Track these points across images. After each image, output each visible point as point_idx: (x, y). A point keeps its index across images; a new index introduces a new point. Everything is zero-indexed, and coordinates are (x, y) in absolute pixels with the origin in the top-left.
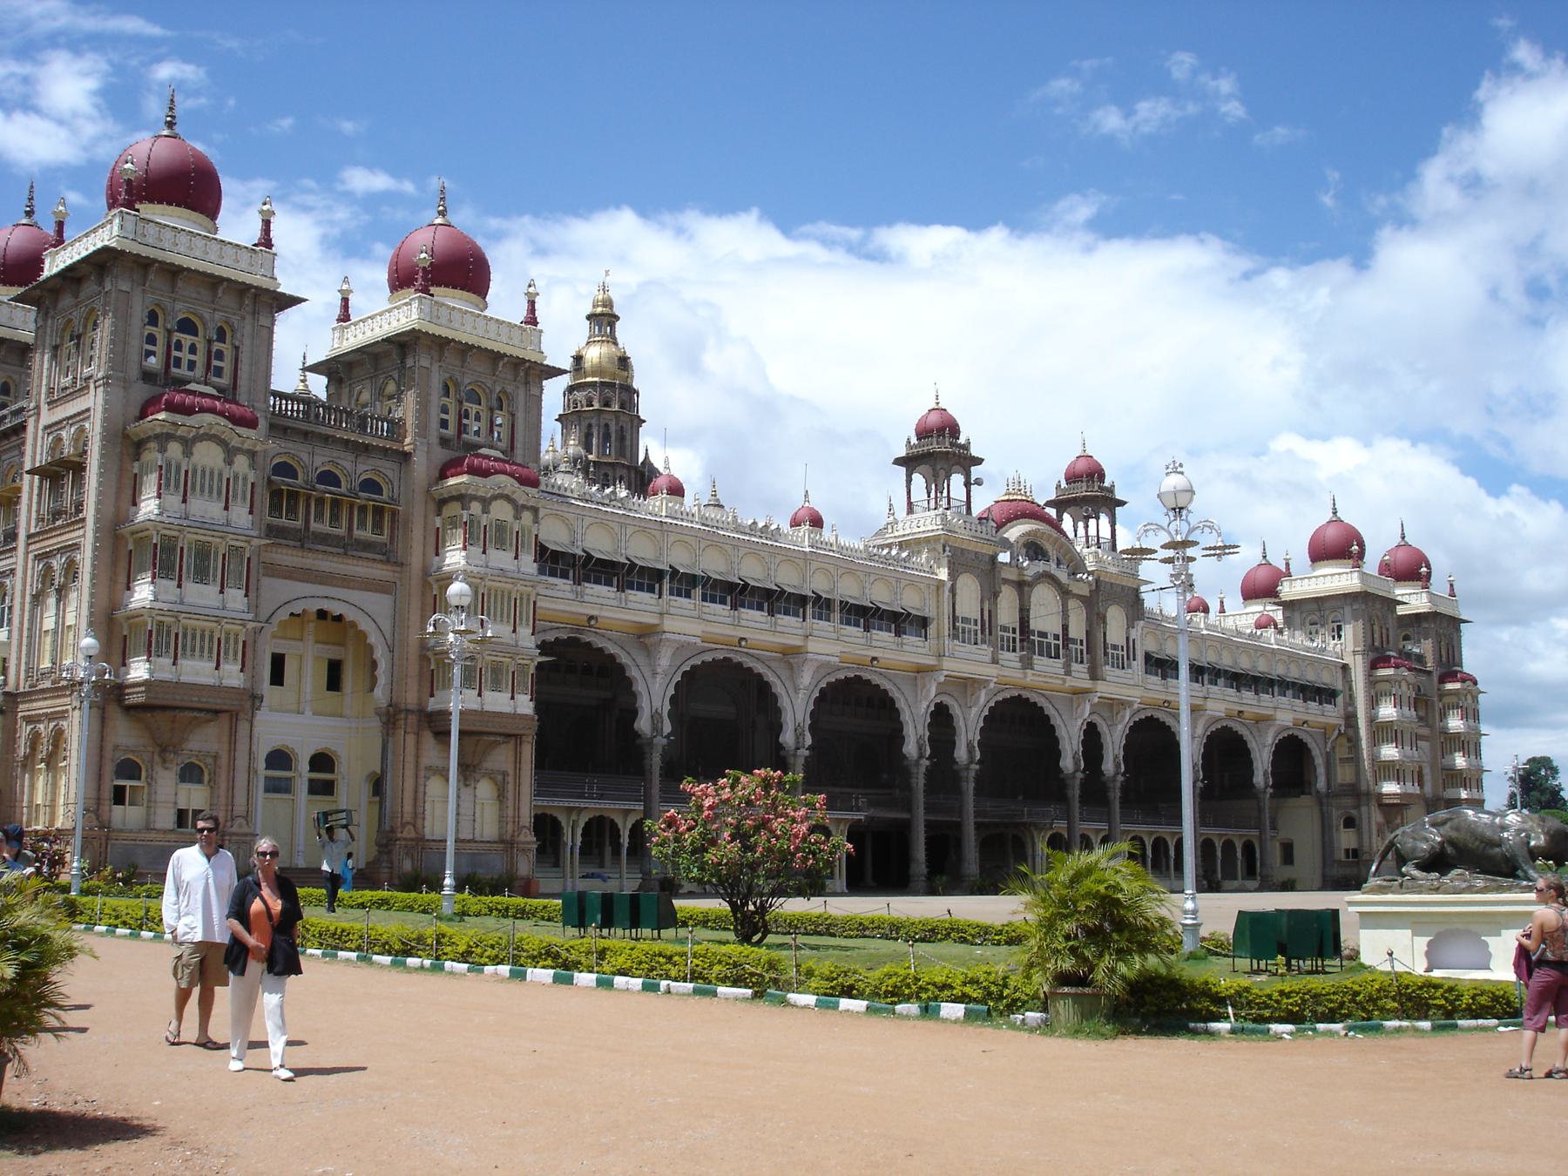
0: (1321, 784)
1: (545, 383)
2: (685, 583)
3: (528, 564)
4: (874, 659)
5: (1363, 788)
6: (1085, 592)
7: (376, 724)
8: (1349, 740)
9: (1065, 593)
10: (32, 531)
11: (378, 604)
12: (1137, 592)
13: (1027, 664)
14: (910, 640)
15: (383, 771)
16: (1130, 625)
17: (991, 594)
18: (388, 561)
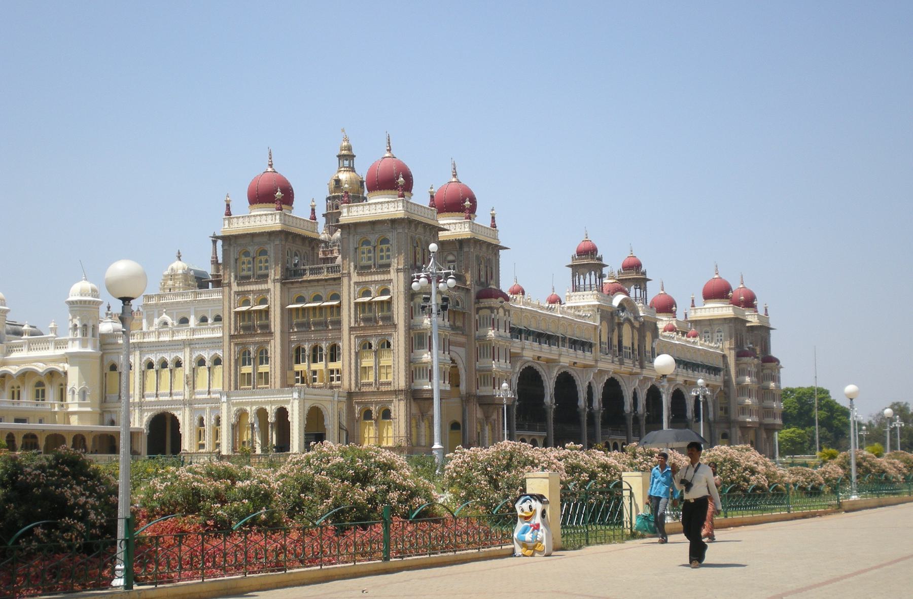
0: (711, 416)
1: (501, 251)
2: (529, 333)
3: (509, 335)
4: (575, 363)
5: (733, 417)
6: (637, 325)
7: (458, 400)
8: (725, 394)
9: (633, 327)
10: (353, 325)
11: (461, 351)
12: (656, 324)
13: (621, 363)
14: (588, 354)
15: (464, 421)
16: (653, 341)
17: (611, 331)
18: (463, 334)
